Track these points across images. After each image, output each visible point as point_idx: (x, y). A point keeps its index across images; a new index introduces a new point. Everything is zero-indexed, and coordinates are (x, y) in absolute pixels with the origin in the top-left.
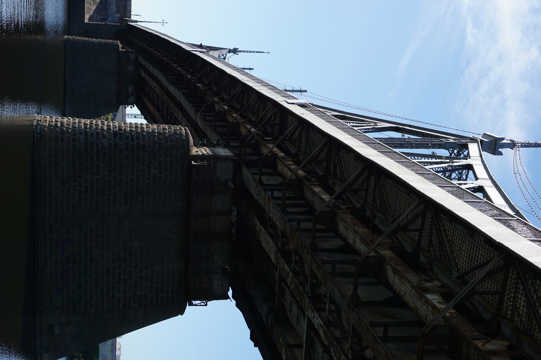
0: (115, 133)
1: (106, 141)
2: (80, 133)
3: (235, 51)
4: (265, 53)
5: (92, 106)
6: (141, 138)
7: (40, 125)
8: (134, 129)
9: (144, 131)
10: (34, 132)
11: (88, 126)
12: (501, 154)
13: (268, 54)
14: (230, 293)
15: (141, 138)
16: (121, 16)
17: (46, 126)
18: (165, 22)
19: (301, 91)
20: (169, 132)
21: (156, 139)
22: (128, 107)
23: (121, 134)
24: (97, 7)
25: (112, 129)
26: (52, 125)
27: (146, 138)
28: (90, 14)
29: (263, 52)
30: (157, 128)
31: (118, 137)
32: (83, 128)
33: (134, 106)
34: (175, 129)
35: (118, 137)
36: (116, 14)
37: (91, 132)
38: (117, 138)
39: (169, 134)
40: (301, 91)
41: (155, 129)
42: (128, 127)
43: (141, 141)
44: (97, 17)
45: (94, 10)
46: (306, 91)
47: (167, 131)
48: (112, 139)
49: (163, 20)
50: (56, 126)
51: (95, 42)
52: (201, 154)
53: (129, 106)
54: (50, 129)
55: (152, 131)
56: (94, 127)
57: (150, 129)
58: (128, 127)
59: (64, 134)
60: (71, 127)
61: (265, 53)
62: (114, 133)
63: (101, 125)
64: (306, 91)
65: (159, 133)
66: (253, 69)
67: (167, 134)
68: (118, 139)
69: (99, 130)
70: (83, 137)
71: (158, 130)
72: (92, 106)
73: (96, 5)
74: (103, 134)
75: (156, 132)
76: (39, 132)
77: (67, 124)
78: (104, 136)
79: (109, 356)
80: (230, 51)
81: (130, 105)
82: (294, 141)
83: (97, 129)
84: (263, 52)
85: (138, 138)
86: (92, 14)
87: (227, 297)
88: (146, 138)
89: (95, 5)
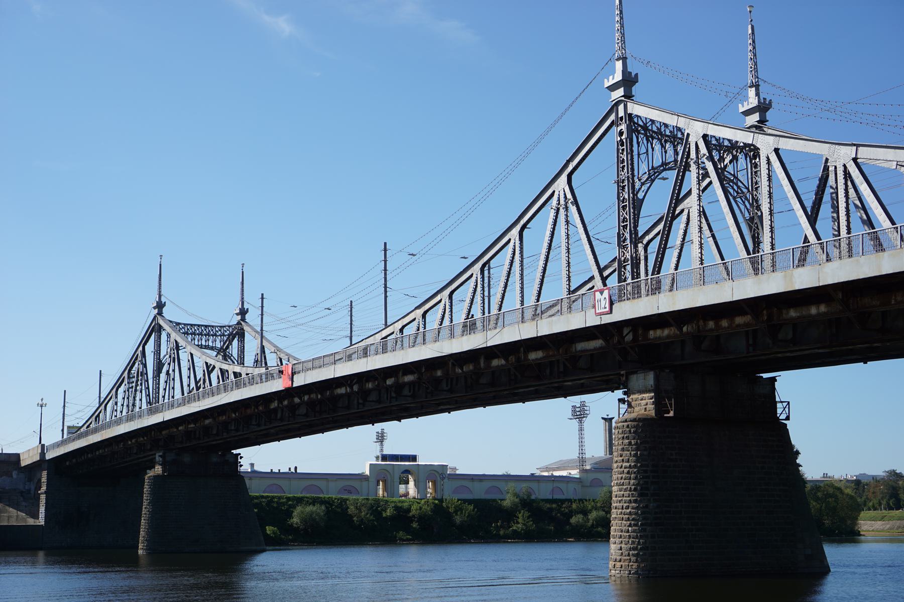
0: (640, 495)
1: (651, 504)
2: (645, 530)
3: (160, 306)
4: (160, 262)
5: (239, 513)
6: (645, 468)
7: (637, 571)
8: (633, 475)
9: (635, 465)
10: (647, 577)
11: (632, 522)
12: (637, 75)
13: (163, 258)
14: (765, 376)
15: (645, 468)
16: (16, 470)
17: (638, 565)
18: (40, 403)
19: (385, 250)
20: (634, 439)
21: (645, 453)
22: (240, 462)
23: (641, 489)
24: (9, 506)
25: (635, 498)
26: (636, 559)
27: (644, 463)
28: (25, 517)
29: (160, 265)
30: (629, 451)
31: (646, 492)
32: (637, 528)
33: (240, 454)
34: (628, 432)
35: (646, 492)
36: (12, 477)
37: (642, 520)
38: (647, 493)
39: (638, 439)
40: (385, 250)
41: (631, 453)
42: (629, 482)
43: (648, 469)
44: (26, 507)
45: (15, 511)
46: (385, 244)
47: (633, 441)
48: (648, 498)
49: (38, 404)
50: (636, 555)
51: (151, 510)
52: (654, 406)
53: (239, 460)
54: (642, 561)
55: (634, 456)
56: (633, 516)
57: (630, 459)
58: (629, 482)
59: (648, 547)
60: (638, 540)
61: (160, 262)
62: (641, 496)
63: (630, 510)
64: (385, 244)
65: (637, 449)
66: (262, 294)
67: (637, 442)
68: (648, 492)
69: (638, 512)
70: (648, 528)
71: (632, 451)
72: (239, 513)
73: (7, 508)
74: (643, 507)
75: (635, 452)
76: (647, 572)
77: (631, 544)
78: (647, 506)
79: (487, 485)
80: (160, 313)
81: (238, 459)
82: (711, 324)
83: (636, 514)
84: (160, 265)
85: (645, 471)
86: (24, 514)
87: (773, 380)
88: (644, 463)
89: (7, 510)
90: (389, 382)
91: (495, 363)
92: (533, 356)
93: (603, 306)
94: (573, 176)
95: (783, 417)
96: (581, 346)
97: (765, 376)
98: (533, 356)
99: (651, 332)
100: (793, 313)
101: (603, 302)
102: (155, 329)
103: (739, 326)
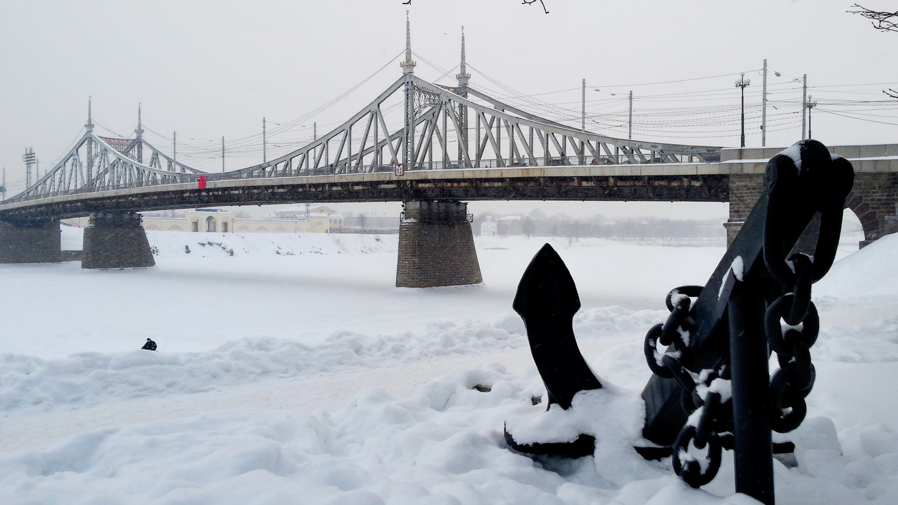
3: (90, 126)
19: (264, 122)
87: (466, 204)
90: (270, 191)
91: (334, 189)
92: (356, 188)
93: (400, 172)
94: (380, 105)
95: (470, 221)
96: (383, 186)
97: (462, 202)
98: (356, 188)
99: (420, 184)
100: (487, 184)
101: (400, 171)
102: (88, 139)
103: (462, 187)
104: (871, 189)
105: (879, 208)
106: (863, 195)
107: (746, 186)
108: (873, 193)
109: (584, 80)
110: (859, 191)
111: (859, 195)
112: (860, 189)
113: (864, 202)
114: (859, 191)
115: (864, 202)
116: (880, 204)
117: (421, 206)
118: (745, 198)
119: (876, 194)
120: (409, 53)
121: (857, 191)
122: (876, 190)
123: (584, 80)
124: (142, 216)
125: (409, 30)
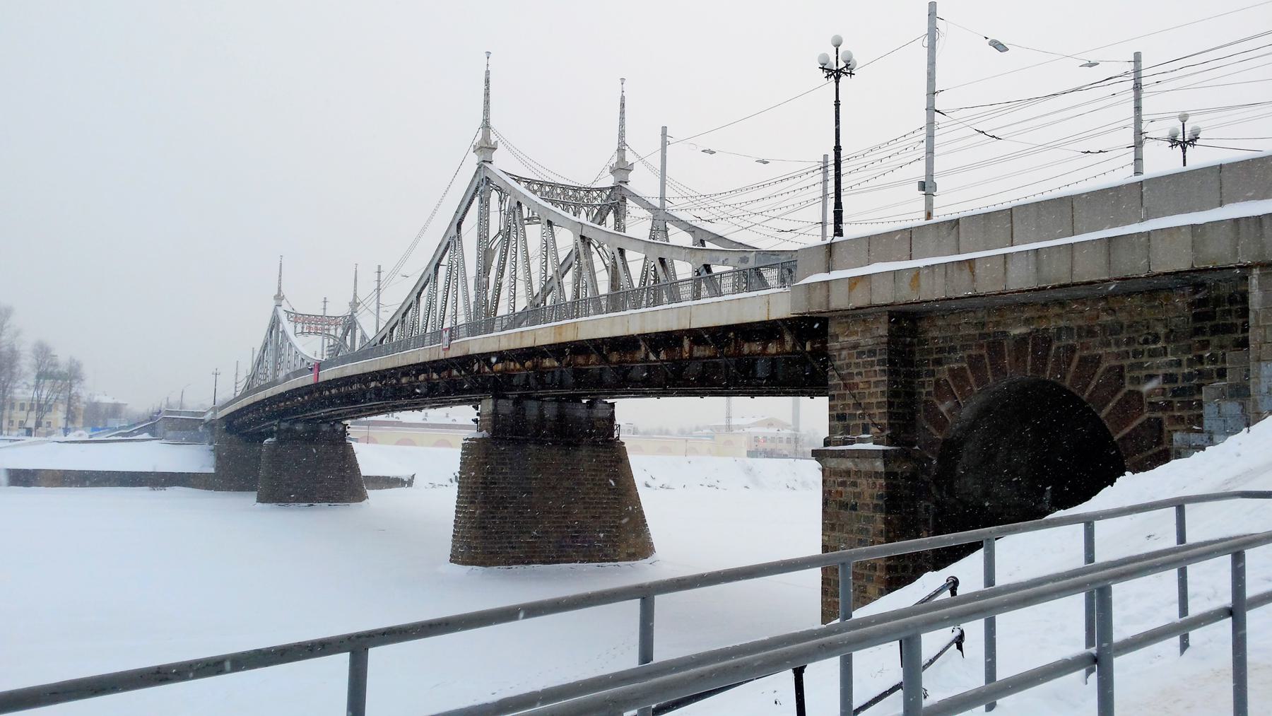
14: (609, 401)
46: (379, 267)
64: (379, 267)
87: (612, 405)
97: (609, 401)
104: (1146, 342)
105: (1169, 406)
106: (1126, 363)
107: (855, 346)
108: (1153, 354)
109: (664, 129)
110: (1114, 349)
111: (1114, 363)
112: (1118, 344)
113: (1128, 387)
114: (1114, 349)
115: (1128, 387)
116: (1175, 393)
117: (495, 405)
118: (857, 379)
119: (1158, 361)
120: (486, 126)
121: (1108, 350)
122: (1159, 345)
123: (664, 129)
124: (349, 428)
125: (624, 112)
